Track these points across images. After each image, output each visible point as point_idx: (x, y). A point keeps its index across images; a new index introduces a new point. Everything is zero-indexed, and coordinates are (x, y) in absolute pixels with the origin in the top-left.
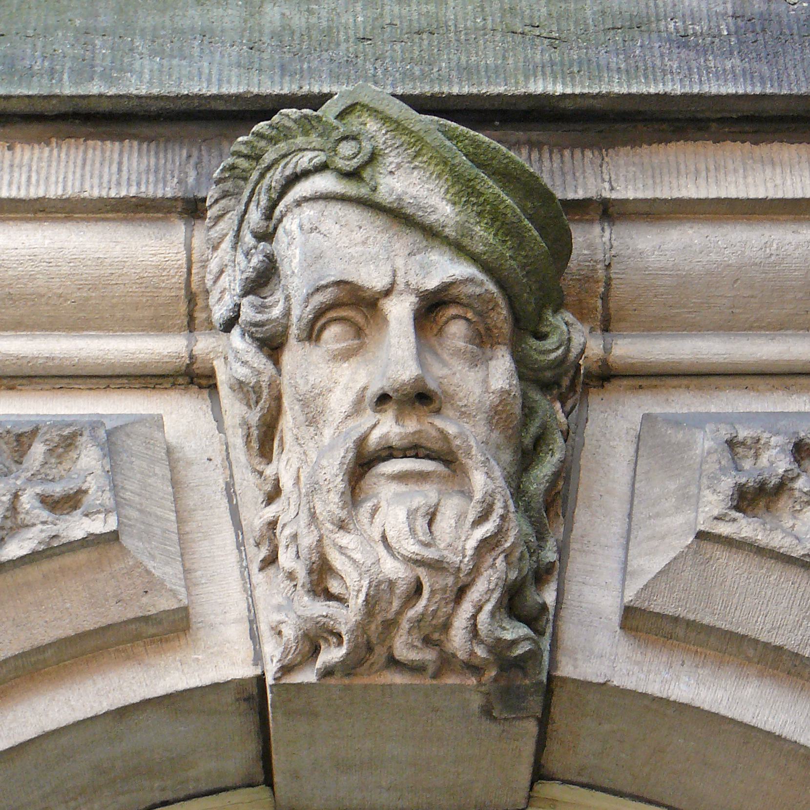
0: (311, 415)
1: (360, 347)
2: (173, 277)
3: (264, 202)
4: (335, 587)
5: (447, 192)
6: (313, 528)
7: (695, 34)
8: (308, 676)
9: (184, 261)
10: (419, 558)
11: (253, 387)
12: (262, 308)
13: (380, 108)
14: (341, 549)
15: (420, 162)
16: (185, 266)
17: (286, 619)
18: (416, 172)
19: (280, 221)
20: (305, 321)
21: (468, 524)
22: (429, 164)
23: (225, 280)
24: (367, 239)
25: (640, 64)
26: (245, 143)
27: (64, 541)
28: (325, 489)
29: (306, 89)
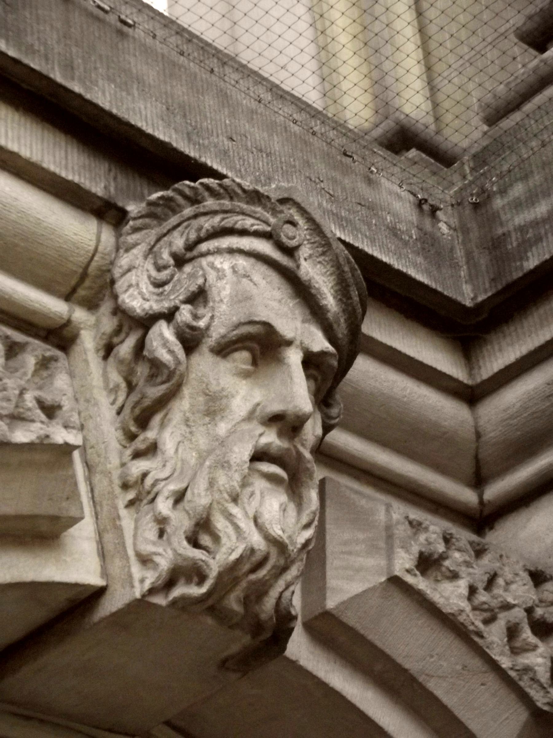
0: (213, 409)
1: (254, 372)
2: (81, 256)
3: (193, 236)
4: (205, 540)
5: (332, 287)
6: (208, 493)
7: (400, 230)
8: (160, 600)
9: (92, 248)
10: (281, 540)
11: (170, 372)
12: (196, 317)
13: (309, 210)
14: (229, 517)
15: (324, 260)
16: (92, 252)
17: (164, 553)
18: (318, 266)
19: (203, 255)
20: (227, 340)
21: (300, 525)
22: (328, 264)
23: (132, 277)
24: (282, 299)
25: (376, 237)
26: (189, 187)
27: (52, 441)
28: (234, 469)
29: (203, 159)
